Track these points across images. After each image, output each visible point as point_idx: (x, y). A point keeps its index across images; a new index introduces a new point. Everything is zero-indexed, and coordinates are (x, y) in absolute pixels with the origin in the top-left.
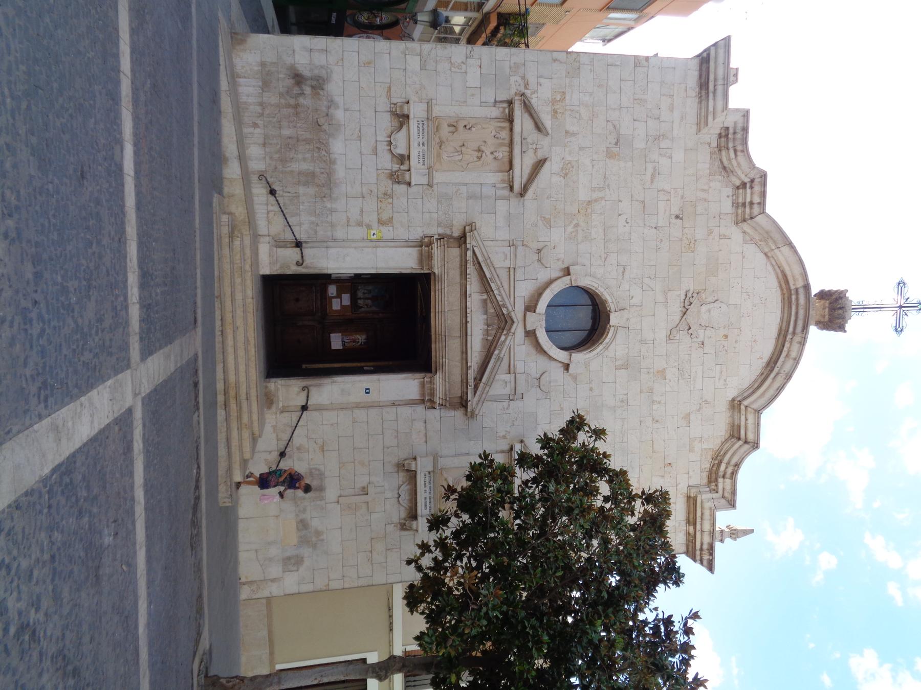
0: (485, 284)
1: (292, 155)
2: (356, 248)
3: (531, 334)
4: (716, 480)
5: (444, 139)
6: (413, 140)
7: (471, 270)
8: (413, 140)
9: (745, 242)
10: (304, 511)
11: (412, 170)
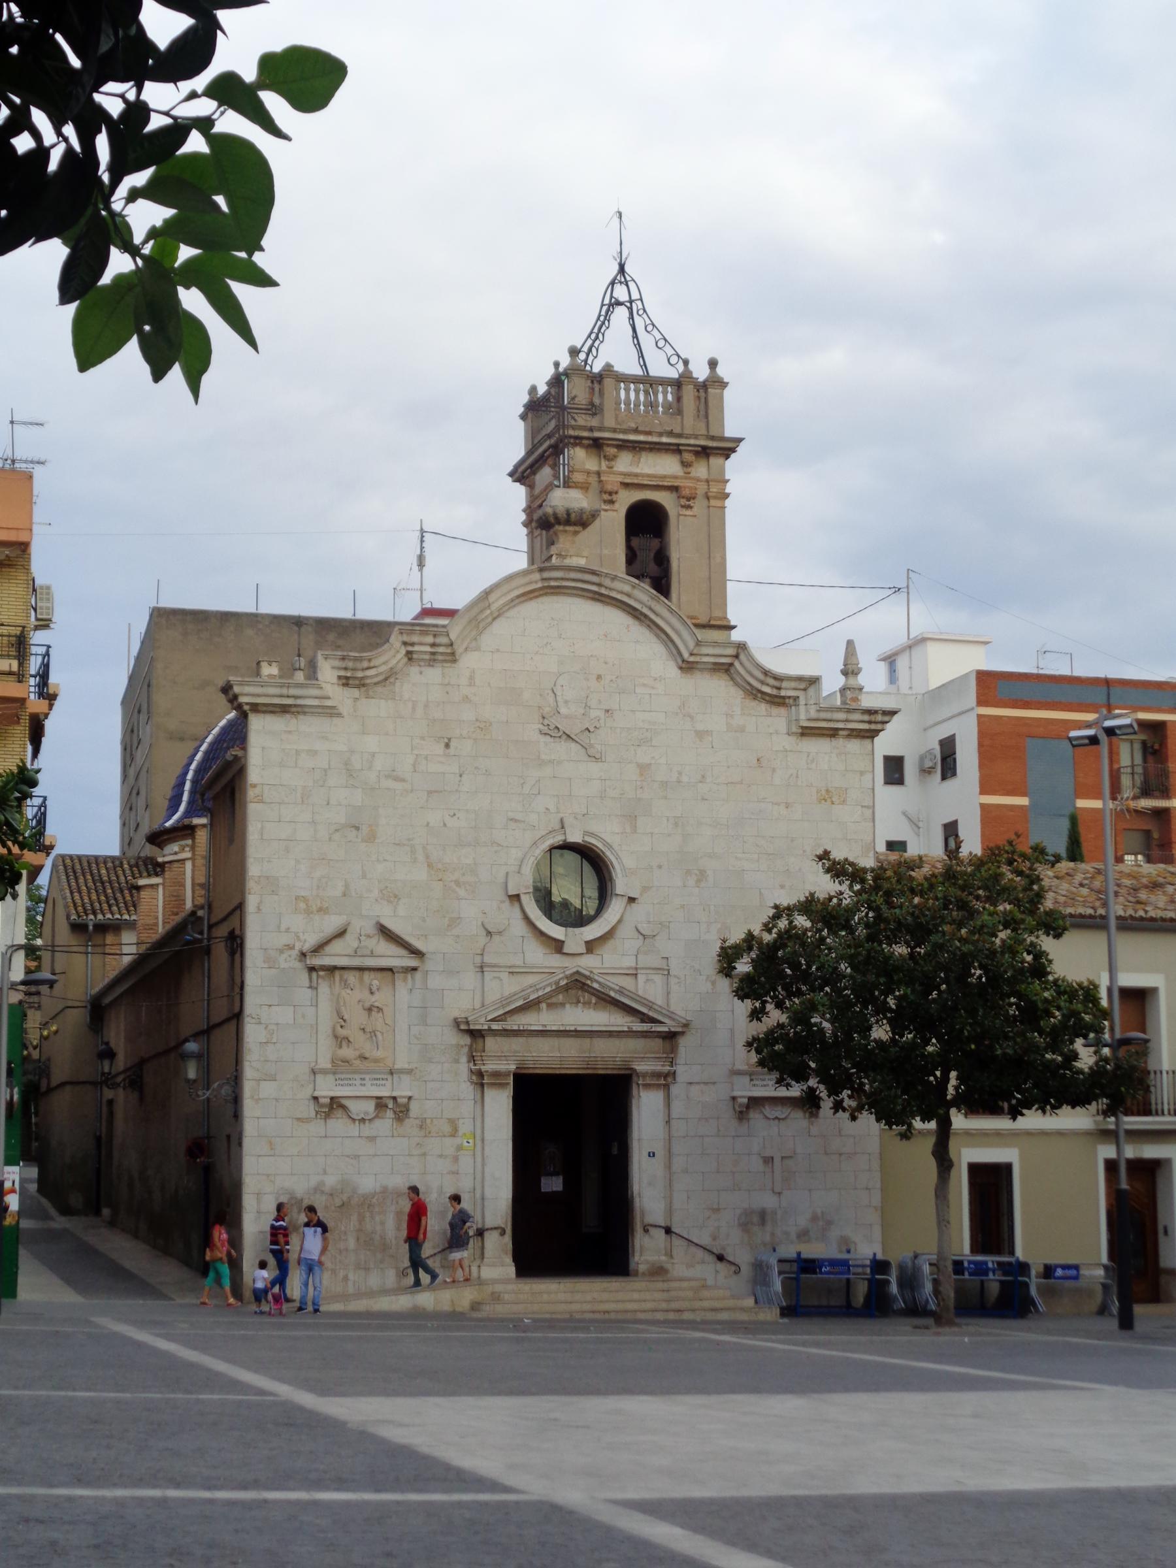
0: (530, 1006)
1: (377, 1237)
2: (483, 1165)
3: (591, 946)
4: (784, 698)
5: (357, 1053)
6: (360, 1090)
7: (514, 1023)
8: (360, 1090)
9: (478, 649)
10: (787, 1233)
11: (394, 1094)
